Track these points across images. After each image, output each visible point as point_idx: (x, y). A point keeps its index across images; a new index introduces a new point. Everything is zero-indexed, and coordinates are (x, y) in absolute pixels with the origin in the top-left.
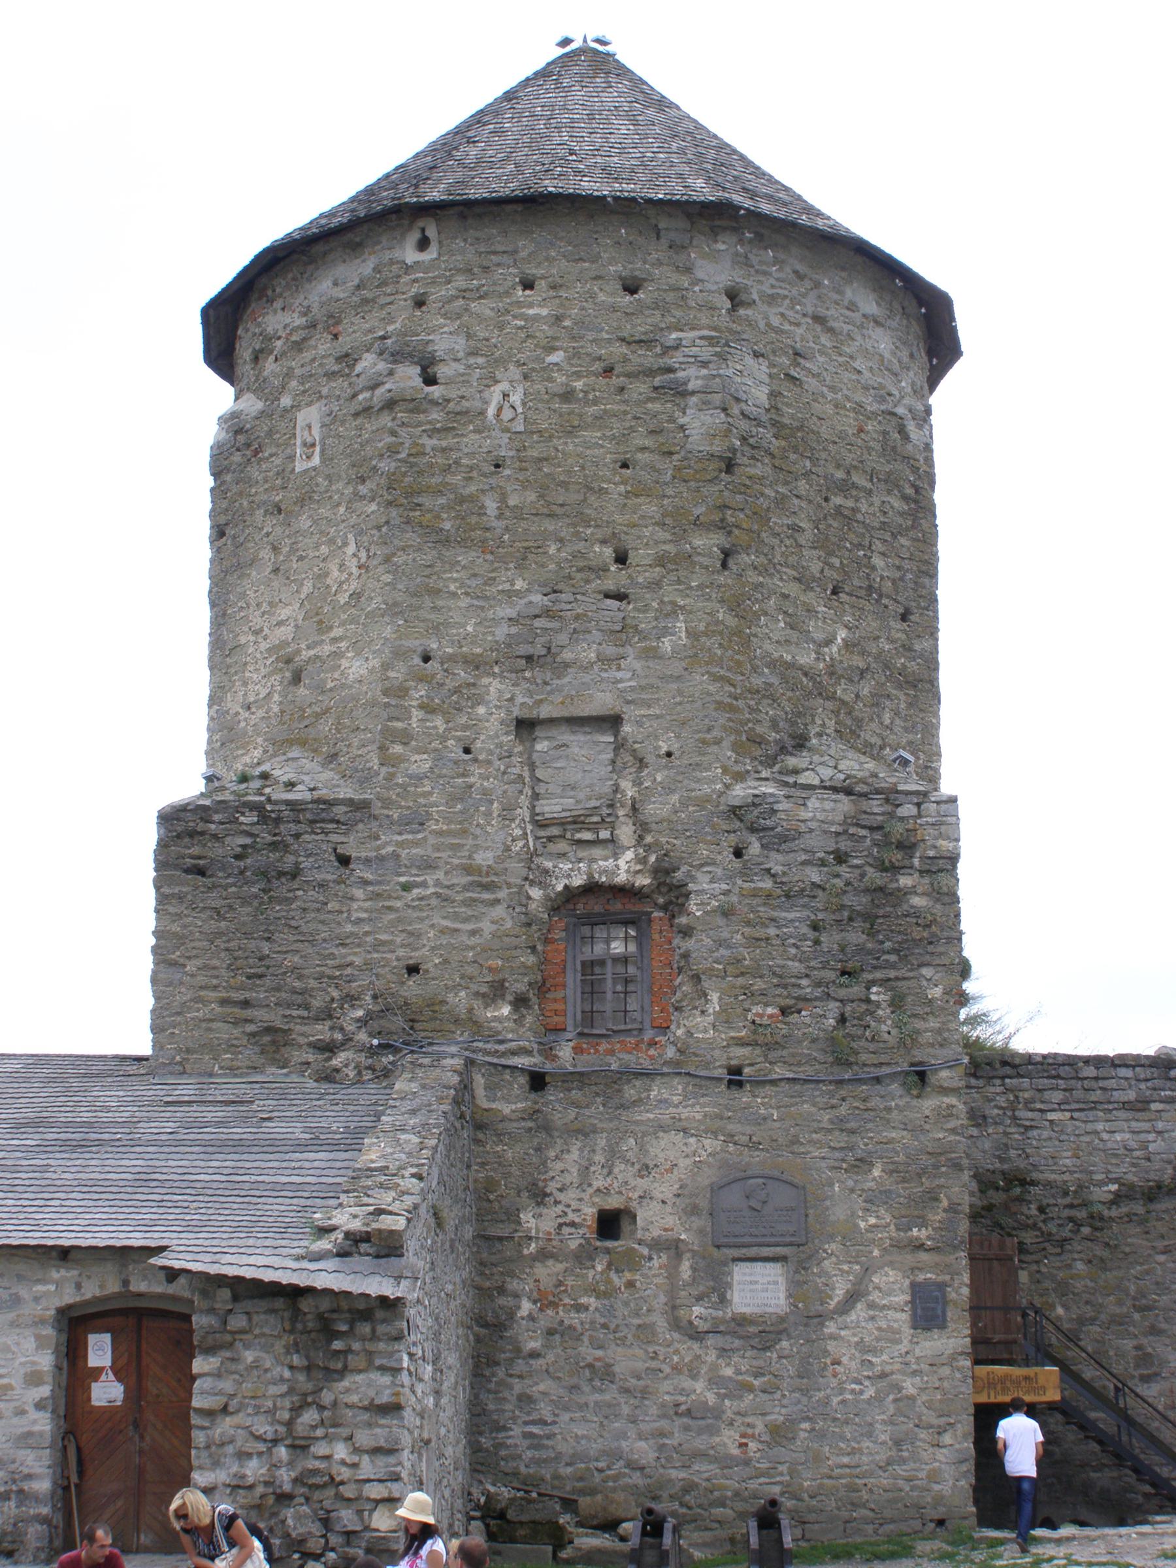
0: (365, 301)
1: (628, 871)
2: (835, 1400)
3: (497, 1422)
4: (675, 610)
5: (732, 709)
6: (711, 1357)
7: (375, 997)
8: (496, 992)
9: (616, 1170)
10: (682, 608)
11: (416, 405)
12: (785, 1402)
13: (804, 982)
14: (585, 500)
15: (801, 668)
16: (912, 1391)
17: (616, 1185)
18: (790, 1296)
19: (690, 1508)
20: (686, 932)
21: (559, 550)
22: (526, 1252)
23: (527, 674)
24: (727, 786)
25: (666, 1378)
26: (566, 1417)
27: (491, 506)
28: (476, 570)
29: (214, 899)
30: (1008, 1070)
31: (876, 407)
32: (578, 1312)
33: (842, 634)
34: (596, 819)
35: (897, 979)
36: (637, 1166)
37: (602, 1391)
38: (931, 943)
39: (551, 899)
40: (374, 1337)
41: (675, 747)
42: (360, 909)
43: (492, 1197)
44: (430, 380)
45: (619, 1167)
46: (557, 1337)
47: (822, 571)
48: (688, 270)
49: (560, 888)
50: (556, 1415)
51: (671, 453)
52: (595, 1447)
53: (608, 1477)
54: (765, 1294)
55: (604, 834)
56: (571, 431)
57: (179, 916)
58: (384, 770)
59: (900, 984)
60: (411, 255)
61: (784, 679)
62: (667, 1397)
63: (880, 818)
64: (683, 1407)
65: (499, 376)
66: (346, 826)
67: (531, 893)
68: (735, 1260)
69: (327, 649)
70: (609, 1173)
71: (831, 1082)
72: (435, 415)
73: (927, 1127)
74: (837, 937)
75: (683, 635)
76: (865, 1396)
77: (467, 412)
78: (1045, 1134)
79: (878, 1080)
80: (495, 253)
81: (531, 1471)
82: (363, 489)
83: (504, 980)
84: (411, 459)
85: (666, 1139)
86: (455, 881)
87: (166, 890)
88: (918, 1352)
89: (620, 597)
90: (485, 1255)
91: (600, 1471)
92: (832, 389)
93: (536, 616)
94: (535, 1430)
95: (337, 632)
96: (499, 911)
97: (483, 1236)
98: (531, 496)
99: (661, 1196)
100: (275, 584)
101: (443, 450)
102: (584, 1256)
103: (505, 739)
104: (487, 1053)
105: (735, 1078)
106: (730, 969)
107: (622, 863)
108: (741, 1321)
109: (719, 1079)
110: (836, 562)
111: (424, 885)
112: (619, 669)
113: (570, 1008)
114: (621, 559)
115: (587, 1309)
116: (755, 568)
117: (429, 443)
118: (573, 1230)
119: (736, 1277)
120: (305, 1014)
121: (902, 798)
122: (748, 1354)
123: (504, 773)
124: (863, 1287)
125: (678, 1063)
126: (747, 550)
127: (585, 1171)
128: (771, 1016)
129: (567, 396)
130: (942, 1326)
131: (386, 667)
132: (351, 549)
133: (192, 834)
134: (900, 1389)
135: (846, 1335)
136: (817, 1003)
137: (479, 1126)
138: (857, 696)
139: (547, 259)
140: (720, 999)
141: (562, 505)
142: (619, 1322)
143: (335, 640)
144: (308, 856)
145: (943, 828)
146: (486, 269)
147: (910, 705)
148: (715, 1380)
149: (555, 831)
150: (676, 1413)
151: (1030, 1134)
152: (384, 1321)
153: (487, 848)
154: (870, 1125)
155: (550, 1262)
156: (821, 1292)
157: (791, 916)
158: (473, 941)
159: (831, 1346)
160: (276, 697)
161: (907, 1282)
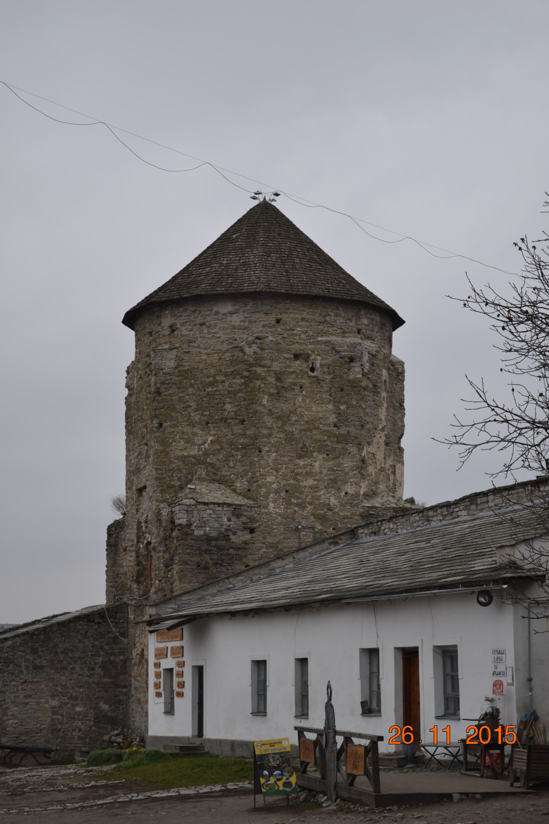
61: (184, 462)
92: (205, 349)
110: (207, 413)
126: (166, 421)
147: (243, 456)
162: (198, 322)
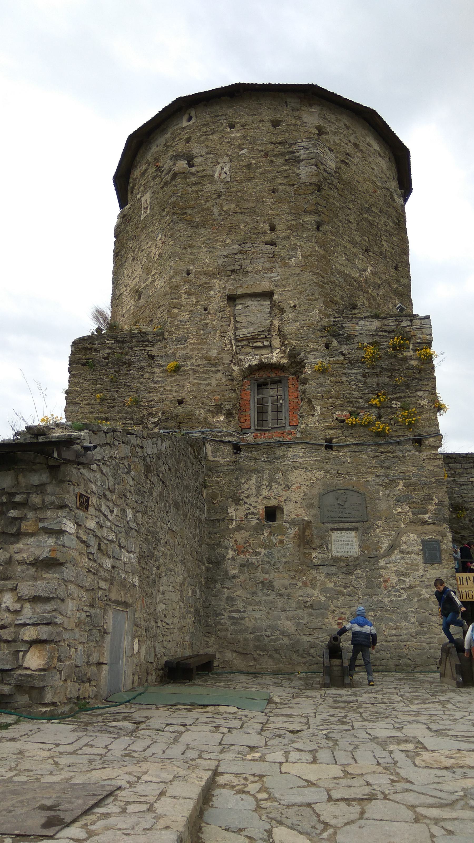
0: (168, 147)
1: (277, 357)
2: (387, 600)
3: (216, 611)
4: (296, 247)
5: (322, 287)
6: (322, 578)
7: (163, 413)
8: (218, 409)
9: (273, 488)
10: (300, 246)
11: (185, 175)
12: (360, 601)
13: (360, 400)
14: (256, 205)
15: (353, 278)
16: (427, 596)
17: (273, 494)
18: (360, 547)
19: (313, 657)
20: (304, 382)
21: (245, 226)
22: (230, 527)
23: (232, 277)
24: (321, 319)
25: (299, 588)
26: (250, 608)
27: (216, 211)
28: (210, 237)
29: (95, 376)
30: (450, 460)
31: (380, 184)
32: (256, 556)
33: (370, 269)
34: (262, 336)
35: (405, 397)
36: (283, 486)
37: (268, 595)
38: (421, 380)
39: (243, 371)
40: (44, 507)
41: (297, 303)
42: (157, 377)
43: (215, 502)
44: (190, 165)
45: (275, 486)
46: (246, 568)
47: (361, 241)
48: (300, 118)
49: (247, 366)
50: (245, 608)
51: (293, 185)
52: (264, 625)
53: (272, 640)
54: (347, 547)
55: (267, 343)
56: (250, 179)
57: (79, 383)
58: (169, 319)
59: (407, 399)
60: (185, 123)
62: (300, 598)
63: (393, 327)
64: (309, 604)
65: (219, 161)
66: (153, 343)
67: (234, 368)
68: (332, 530)
69: (150, 280)
70: (270, 489)
71: (375, 445)
72: (193, 179)
73: (424, 465)
74: (375, 380)
75: (300, 257)
76: (402, 598)
77: (206, 176)
78: (470, 487)
79: (398, 443)
80: (218, 116)
81: (233, 636)
82: (164, 213)
83: (221, 404)
84: (183, 196)
85: (296, 472)
86: (199, 363)
87: (73, 372)
88: (428, 577)
89: (273, 244)
90: (211, 529)
91: (268, 636)
93: (236, 254)
94: (235, 615)
95: (153, 272)
96: (219, 375)
97: (210, 520)
98: (233, 206)
99: (295, 499)
100: (133, 265)
101: (197, 191)
102: (258, 529)
103: (222, 303)
104: (214, 436)
105: (329, 445)
106: (325, 395)
107: (275, 354)
108: (336, 559)
109: (321, 445)
110: (367, 239)
111: (186, 366)
112: (272, 272)
113: (252, 420)
114: (273, 228)
115: (260, 554)
116: (332, 233)
117: (190, 189)
118: (253, 516)
119: (333, 538)
120: (132, 422)
121: (403, 318)
122: (340, 576)
123: (222, 318)
124: (397, 542)
125: (301, 438)
126: (328, 224)
127: (258, 489)
128: (345, 416)
129: (249, 166)
130: (440, 563)
131: (171, 278)
132: (160, 236)
133: (86, 349)
134: (420, 595)
135: (390, 568)
136: (367, 410)
137: (210, 469)
138: (378, 294)
139: (240, 116)
140: (321, 408)
141: (246, 209)
142: (276, 560)
143: (153, 275)
144: (137, 356)
145: (424, 330)
146: (214, 123)
148: (324, 590)
149: (245, 343)
150: (305, 607)
151: (463, 487)
152: (53, 494)
153: (214, 349)
154: (396, 464)
155: (242, 532)
156: (376, 545)
157: (353, 371)
158: (207, 388)
159: (382, 572)
160: (132, 307)
161: (420, 540)
162: (352, 141)
